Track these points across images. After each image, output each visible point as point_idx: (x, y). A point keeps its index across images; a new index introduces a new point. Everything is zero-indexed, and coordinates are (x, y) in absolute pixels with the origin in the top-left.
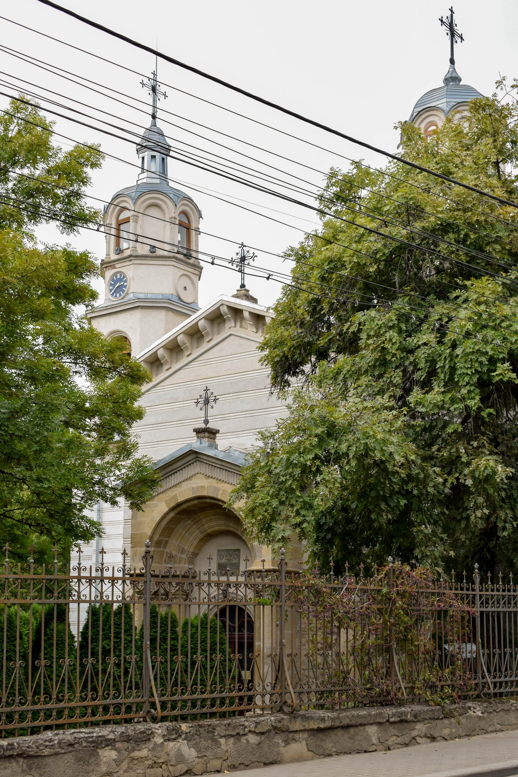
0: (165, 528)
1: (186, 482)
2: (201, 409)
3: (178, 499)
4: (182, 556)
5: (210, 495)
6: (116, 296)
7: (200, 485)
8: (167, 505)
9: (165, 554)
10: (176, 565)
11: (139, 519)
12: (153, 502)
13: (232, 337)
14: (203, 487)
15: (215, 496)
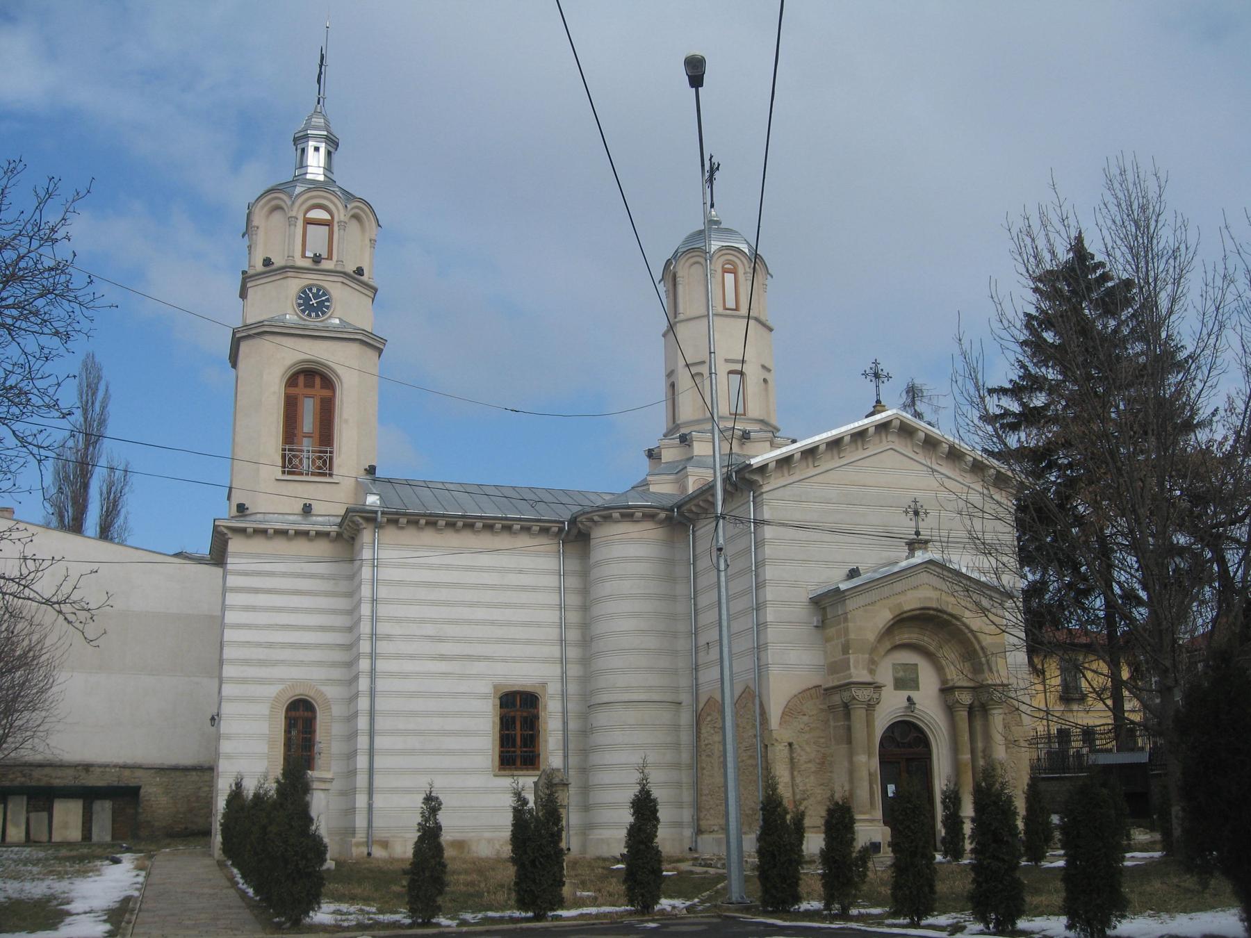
1: (911, 591)
2: (911, 520)
6: (309, 315)
13: (893, 452)
14: (930, 599)
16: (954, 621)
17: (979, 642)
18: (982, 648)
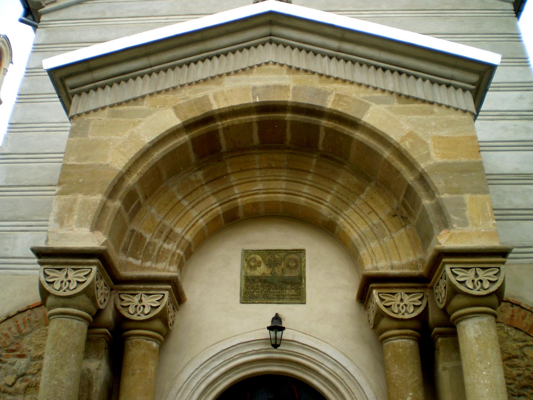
0: (155, 169)
1: (233, 77)
3: (210, 105)
4: (166, 246)
5: (305, 99)
7: (276, 82)
8: (178, 115)
9: (128, 233)
10: (148, 264)
11: (90, 137)
12: (136, 107)
15: (316, 102)
16: (346, 130)
17: (411, 165)
18: (422, 178)
